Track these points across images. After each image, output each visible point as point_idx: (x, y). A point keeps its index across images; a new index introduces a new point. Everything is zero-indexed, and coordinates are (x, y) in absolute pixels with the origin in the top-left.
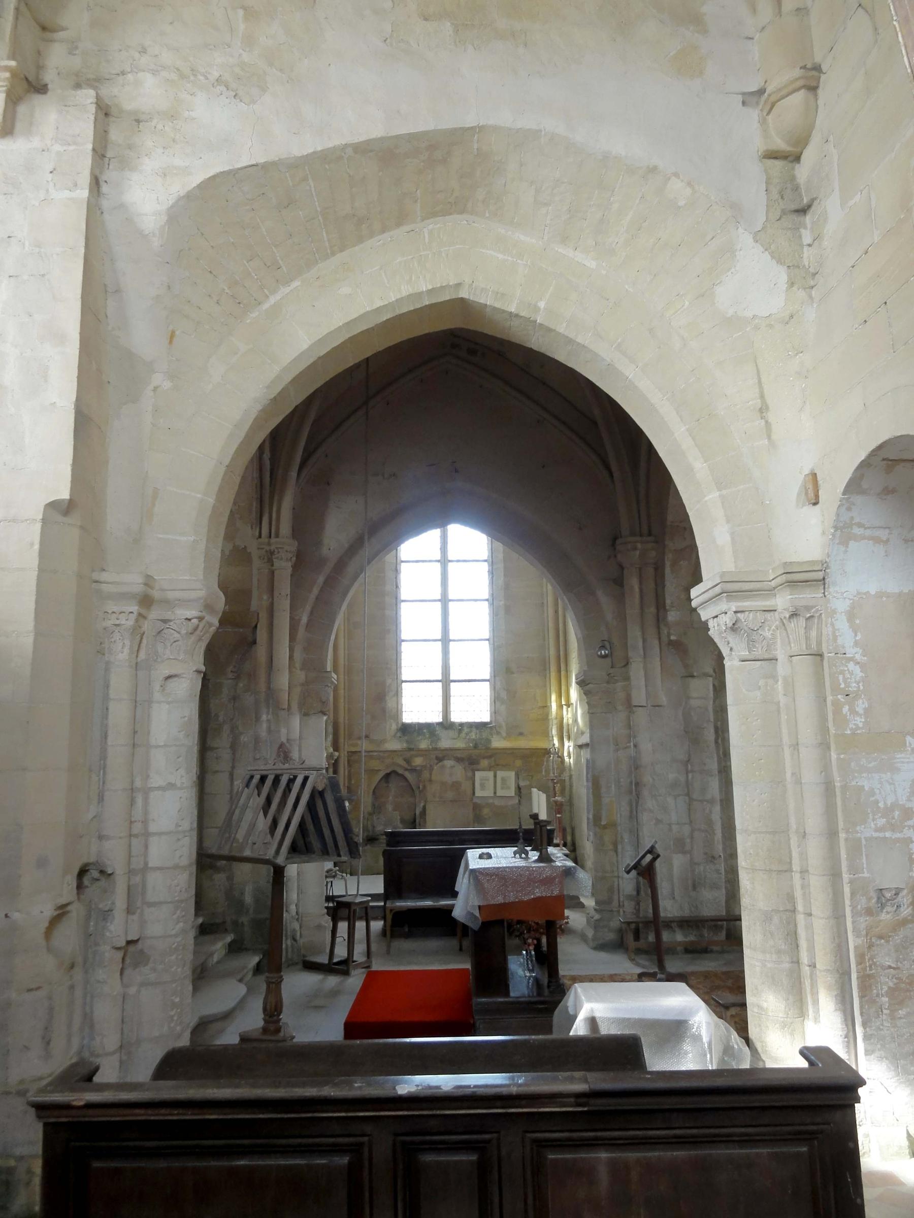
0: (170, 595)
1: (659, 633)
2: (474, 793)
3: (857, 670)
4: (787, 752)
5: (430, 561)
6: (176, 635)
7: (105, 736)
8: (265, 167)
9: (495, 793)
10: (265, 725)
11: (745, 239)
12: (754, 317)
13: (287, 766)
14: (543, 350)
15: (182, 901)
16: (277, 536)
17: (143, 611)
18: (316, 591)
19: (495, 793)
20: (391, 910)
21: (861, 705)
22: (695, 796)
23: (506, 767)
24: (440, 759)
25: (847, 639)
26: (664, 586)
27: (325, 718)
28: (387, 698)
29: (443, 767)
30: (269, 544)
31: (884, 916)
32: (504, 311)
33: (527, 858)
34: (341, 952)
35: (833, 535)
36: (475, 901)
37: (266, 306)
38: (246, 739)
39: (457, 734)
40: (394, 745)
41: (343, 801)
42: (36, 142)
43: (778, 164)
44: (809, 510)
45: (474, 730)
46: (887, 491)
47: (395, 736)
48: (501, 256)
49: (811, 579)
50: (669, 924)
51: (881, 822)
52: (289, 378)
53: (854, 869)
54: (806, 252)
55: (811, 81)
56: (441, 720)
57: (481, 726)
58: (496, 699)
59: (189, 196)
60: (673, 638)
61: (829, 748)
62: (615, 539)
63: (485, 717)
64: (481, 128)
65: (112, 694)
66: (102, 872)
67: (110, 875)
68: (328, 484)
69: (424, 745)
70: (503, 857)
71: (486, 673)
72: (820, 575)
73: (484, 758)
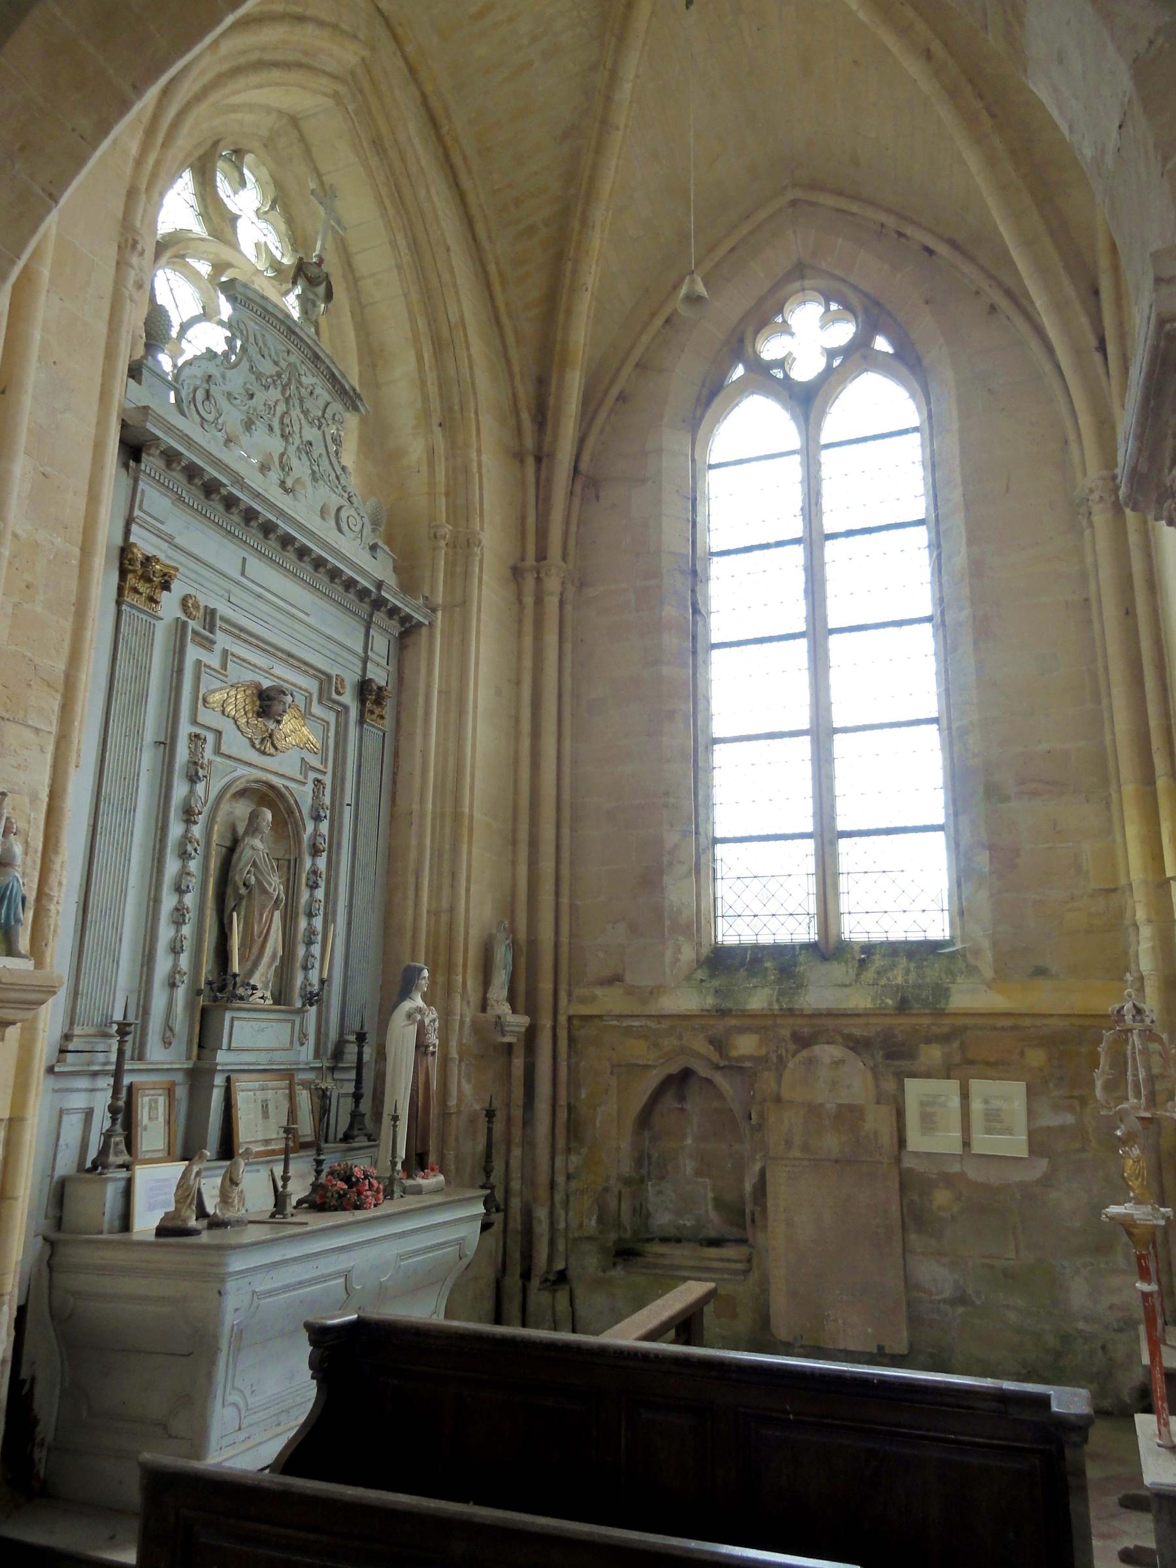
2: (902, 1142)
5: (779, 544)
9: (966, 1144)
19: (966, 1144)
23: (997, 1068)
24: (803, 1041)
29: (811, 1062)
39: (852, 973)
40: (686, 1001)
45: (903, 962)
47: (688, 978)
56: (814, 937)
57: (921, 952)
58: (962, 876)
63: (938, 928)
69: (758, 1000)
71: (935, 808)
73: (929, 1041)
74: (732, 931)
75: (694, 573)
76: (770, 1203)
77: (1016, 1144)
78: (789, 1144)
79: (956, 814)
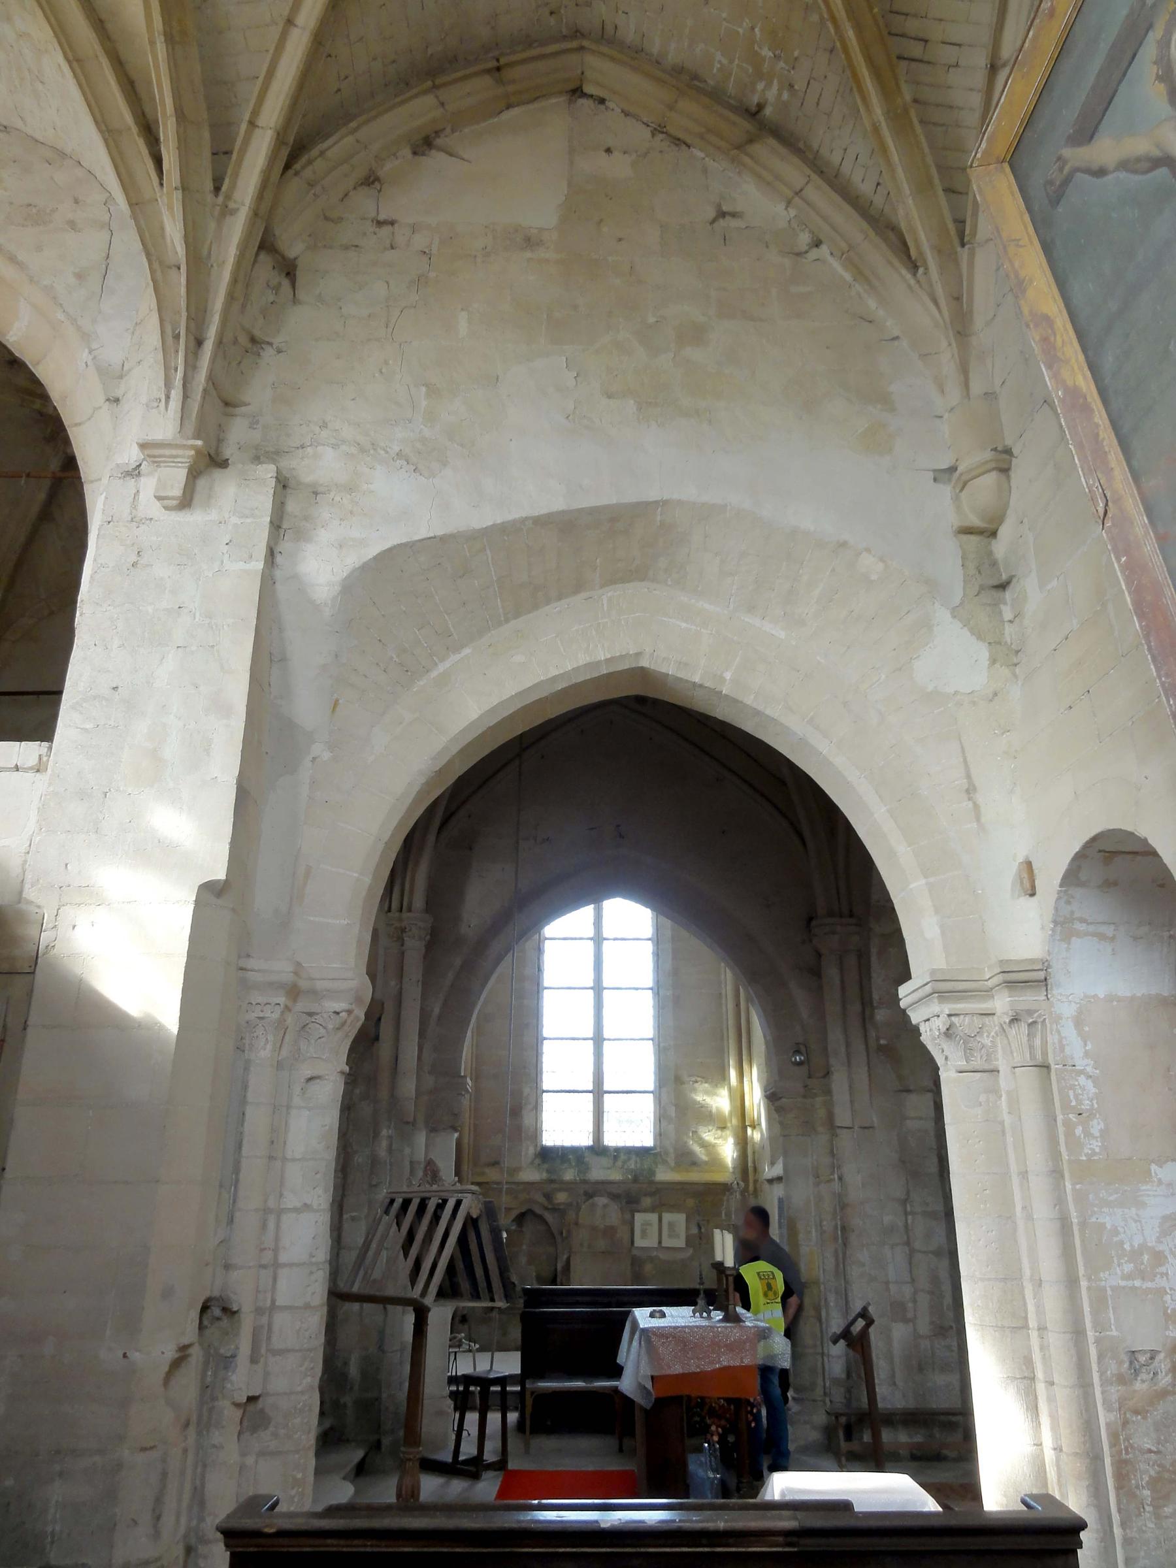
0: (320, 985)
1: (866, 1036)
2: (632, 1242)
3: (1089, 1084)
4: (1015, 1181)
6: (322, 1031)
7: (239, 1146)
8: (443, 539)
9: (660, 1242)
10: (384, 1143)
11: (942, 615)
12: (956, 692)
13: (435, 1187)
14: (728, 720)
15: (310, 1350)
16: (410, 910)
17: (289, 1004)
18: (450, 975)
19: (660, 1242)
20: (532, 1393)
21: (1096, 1126)
22: (917, 1245)
23: (674, 1208)
24: (589, 1196)
25: (1076, 1049)
26: (870, 978)
27: (456, 1135)
28: (524, 1112)
29: (594, 1205)
30: (400, 920)
31: (1138, 1386)
32: (687, 681)
33: (709, 1317)
34: (468, 1450)
35: (1053, 930)
36: (646, 1370)
37: (434, 674)
38: (360, 1160)
39: (611, 1162)
40: (531, 1175)
41: (500, 1231)
42: (213, 515)
43: (974, 539)
44: (1026, 902)
45: (634, 1157)
46: (1109, 884)
47: (532, 1163)
48: (684, 625)
49: (1031, 979)
50: (892, 1419)
51: (1128, 1267)
52: (455, 749)
53: (1099, 1326)
54: (1008, 629)
55: (1003, 462)
56: (590, 1143)
57: (642, 1152)
58: (661, 1117)
59: (365, 568)
60: (882, 1042)
61: (1063, 1176)
62: (810, 919)
63: (648, 1141)
64: (665, 503)
65: (250, 1097)
66: (225, 1310)
67: (235, 1312)
68: (471, 849)
69: (569, 1175)
70: (679, 1316)
71: (649, 1083)
72: (1041, 975)
73: (645, 1195)
74: (550, 1139)
75: (539, 949)
76: (572, 1274)
77: (681, 1243)
78: (581, 1245)
79: (660, 1087)
